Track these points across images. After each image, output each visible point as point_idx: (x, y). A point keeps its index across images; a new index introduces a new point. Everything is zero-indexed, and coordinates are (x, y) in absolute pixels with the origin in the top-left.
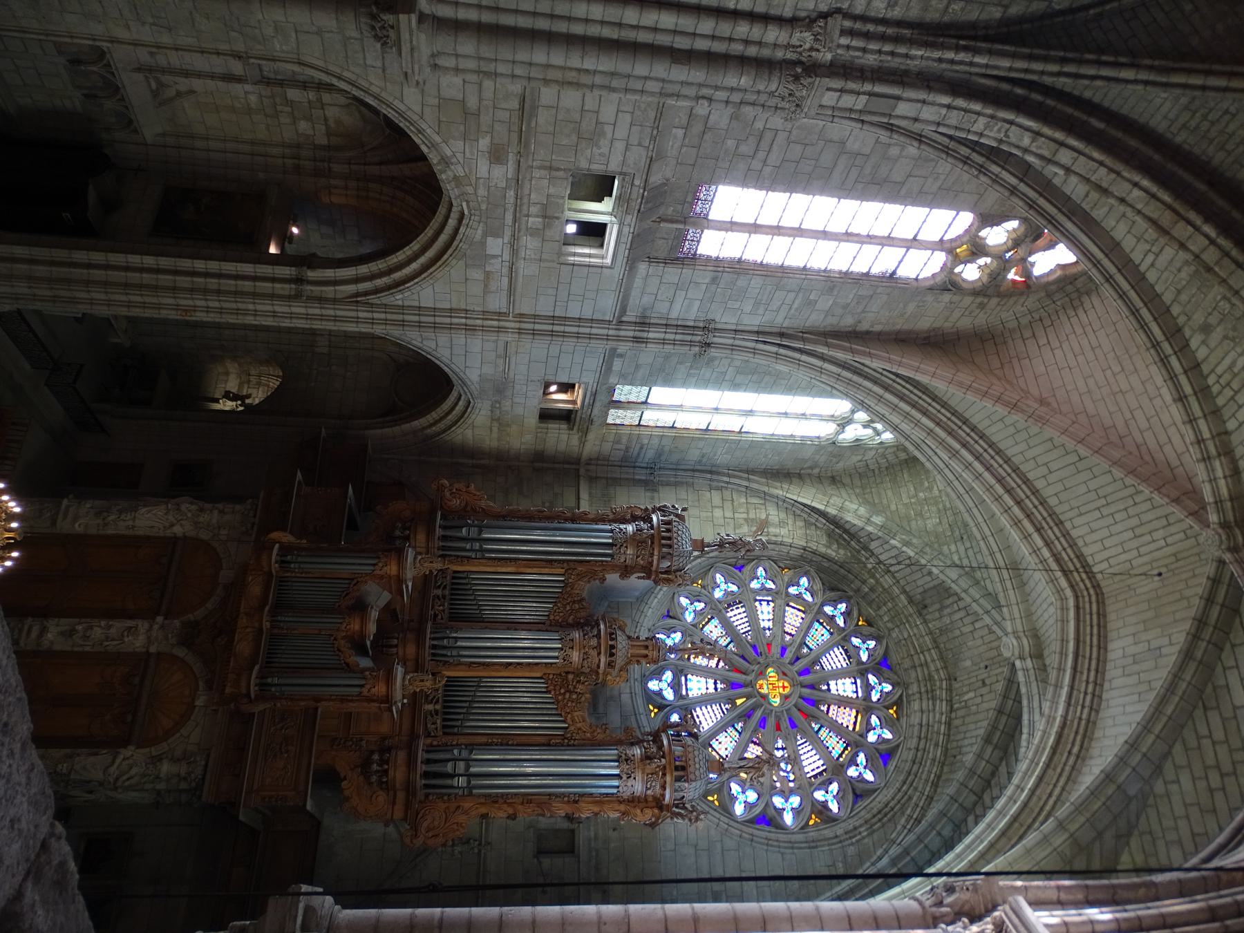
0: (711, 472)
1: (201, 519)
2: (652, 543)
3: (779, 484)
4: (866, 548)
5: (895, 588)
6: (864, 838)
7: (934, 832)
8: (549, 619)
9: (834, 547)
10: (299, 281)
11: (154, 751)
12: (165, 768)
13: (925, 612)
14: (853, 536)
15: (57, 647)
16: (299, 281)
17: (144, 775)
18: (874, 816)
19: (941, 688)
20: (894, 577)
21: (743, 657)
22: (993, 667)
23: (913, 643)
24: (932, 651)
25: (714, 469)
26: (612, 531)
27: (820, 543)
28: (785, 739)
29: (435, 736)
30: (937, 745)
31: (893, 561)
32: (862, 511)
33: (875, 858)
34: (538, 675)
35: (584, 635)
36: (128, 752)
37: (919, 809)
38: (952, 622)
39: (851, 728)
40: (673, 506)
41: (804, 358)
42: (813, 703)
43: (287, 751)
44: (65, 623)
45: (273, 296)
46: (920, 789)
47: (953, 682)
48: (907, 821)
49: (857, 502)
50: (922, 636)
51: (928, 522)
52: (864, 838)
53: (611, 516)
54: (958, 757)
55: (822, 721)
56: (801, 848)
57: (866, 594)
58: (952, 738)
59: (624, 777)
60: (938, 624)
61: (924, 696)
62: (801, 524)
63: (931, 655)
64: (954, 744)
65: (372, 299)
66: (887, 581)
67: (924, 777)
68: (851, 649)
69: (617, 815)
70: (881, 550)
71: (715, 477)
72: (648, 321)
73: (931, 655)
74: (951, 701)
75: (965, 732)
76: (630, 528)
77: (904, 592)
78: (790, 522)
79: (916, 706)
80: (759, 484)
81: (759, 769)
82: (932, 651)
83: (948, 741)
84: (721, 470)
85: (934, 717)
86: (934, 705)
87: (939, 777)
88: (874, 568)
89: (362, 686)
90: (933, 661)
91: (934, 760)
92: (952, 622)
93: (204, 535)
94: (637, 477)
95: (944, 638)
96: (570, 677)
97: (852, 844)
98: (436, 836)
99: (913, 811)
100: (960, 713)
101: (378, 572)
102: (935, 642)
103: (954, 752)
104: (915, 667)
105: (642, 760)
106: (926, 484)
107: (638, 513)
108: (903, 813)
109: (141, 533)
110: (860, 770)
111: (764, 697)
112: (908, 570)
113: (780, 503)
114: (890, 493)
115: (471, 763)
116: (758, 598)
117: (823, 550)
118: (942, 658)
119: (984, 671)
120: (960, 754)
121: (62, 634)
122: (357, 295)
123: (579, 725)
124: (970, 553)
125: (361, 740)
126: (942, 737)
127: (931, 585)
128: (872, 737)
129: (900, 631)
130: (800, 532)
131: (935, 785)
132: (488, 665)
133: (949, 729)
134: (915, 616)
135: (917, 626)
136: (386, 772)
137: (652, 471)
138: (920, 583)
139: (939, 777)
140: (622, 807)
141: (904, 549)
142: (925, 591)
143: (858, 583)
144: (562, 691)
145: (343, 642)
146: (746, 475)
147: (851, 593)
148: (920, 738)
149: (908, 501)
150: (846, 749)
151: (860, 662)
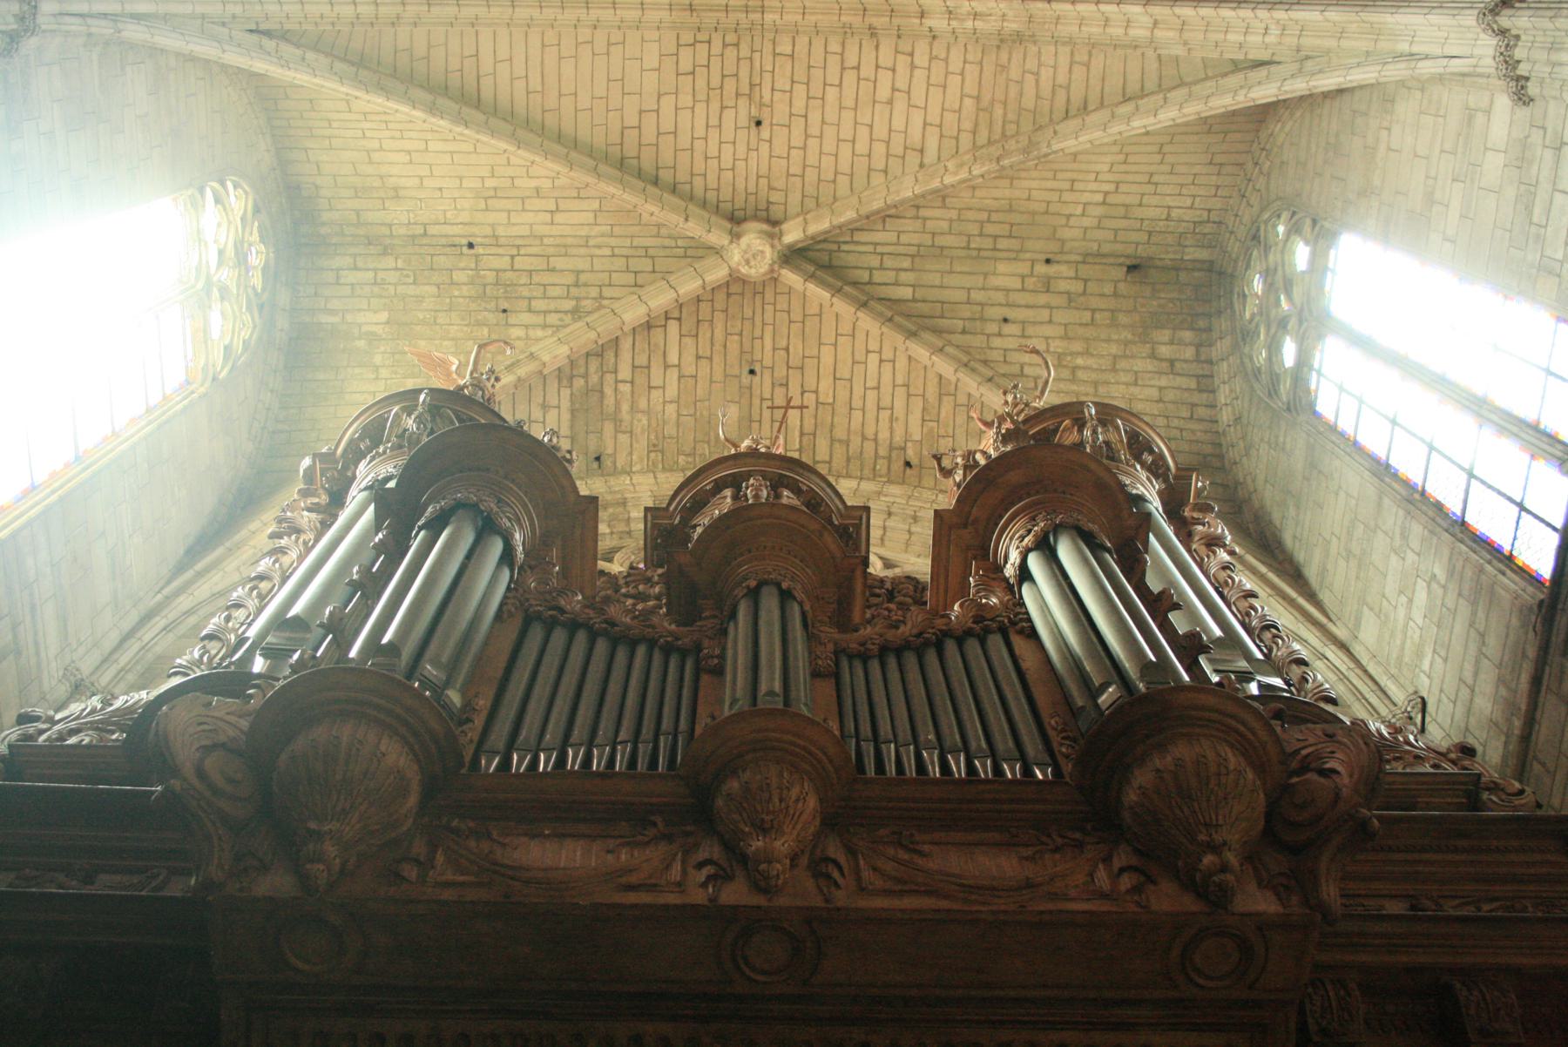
13: (607, 462)
22: (758, 356)
38: (648, 412)
54: (911, 454)
75: (864, 438)
103: (898, 466)
106: (361, 344)
119: (757, 379)
120: (904, 449)
124: (539, 305)
146: (189, 574)
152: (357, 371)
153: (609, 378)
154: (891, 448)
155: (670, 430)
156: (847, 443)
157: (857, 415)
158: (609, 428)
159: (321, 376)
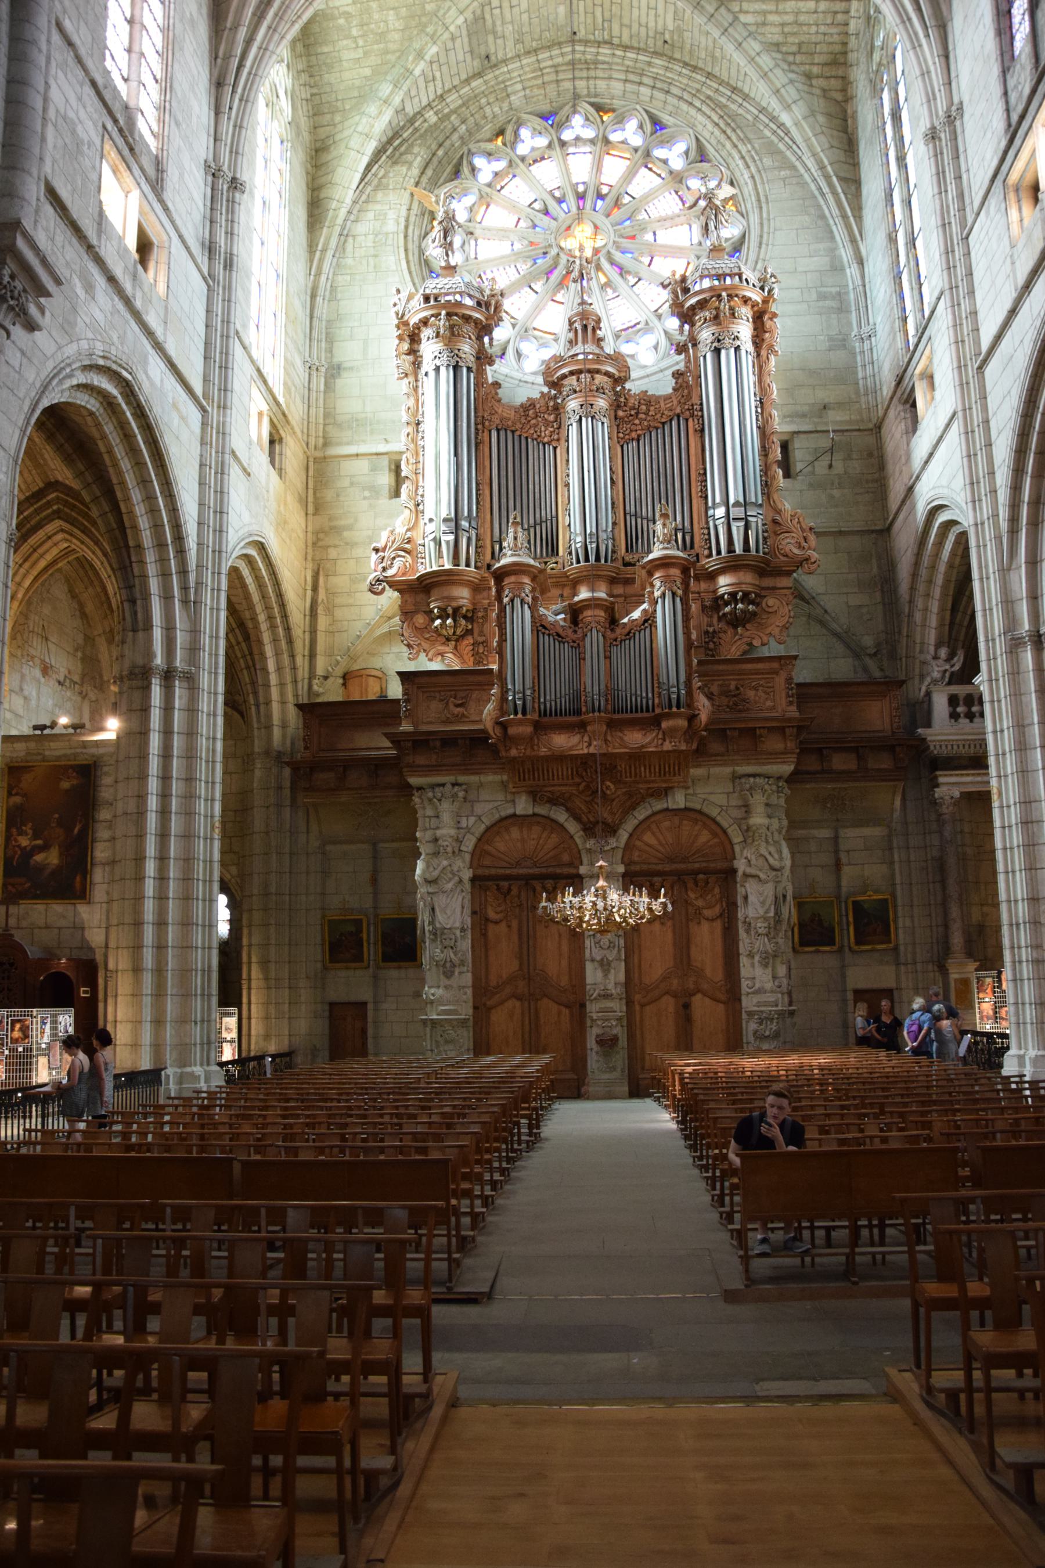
0: (313, 296)
1: (449, 849)
2: (456, 315)
3: (331, 213)
4: (412, 121)
5: (462, 92)
6: (753, 148)
7: (757, 59)
8: (549, 443)
9: (409, 157)
10: (168, 676)
11: (737, 838)
12: (758, 819)
13: (493, 58)
14: (396, 135)
15: (622, 977)
16: (168, 676)
17: (767, 842)
18: (729, 138)
19: (584, 53)
20: (449, 91)
21: (551, 272)
23: (529, 80)
24: (540, 57)
25: (309, 292)
26: (437, 369)
27: (406, 174)
28: (643, 230)
29: (697, 555)
30: (649, 64)
31: (431, 89)
32: (372, 109)
33: (773, 138)
34: (619, 449)
35: (575, 392)
36: (741, 865)
37: (721, 88)
38: (512, 22)
39: (628, 162)
40: (395, 305)
41: (248, 63)
42: (601, 196)
43: (737, 689)
44: (593, 975)
45: (192, 710)
46: (698, 86)
47: (577, 38)
48: (734, 102)
49: (357, 118)
50: (522, 67)
51: (391, 27)
52: (753, 148)
53: (411, 379)
54: (667, 37)
55: (622, 191)
56: (768, 212)
57: (467, 130)
58: (642, 45)
59: (738, 343)
60: (510, 44)
61: (592, 73)
62: (380, 195)
63: (544, 60)
64: (651, 42)
65: (192, 578)
66: (453, 100)
67: (685, 81)
68: (537, 155)
69: (772, 358)
70: (416, 100)
71: (320, 292)
72: (207, 243)
73: (544, 60)
74: (599, 42)
75: (640, 25)
76: (430, 349)
77: (467, 81)
78: (378, 207)
79: (602, 85)
80: (331, 236)
81: (717, 208)
82: (540, 57)
83: (645, 51)
84: (310, 285)
85: (617, 64)
86: (604, 63)
87: (686, 64)
88: (436, 113)
89: (674, 594)
90: (551, 58)
91: (667, 68)
92: (512, 22)
93: (469, 843)
94: (322, 387)
95: (527, 38)
96: (621, 413)
97: (761, 160)
98: (805, 539)
99: (723, 95)
100: (616, 31)
101: (529, 599)
102: (529, 52)
103: (660, 43)
104: (557, 81)
105: (719, 324)
106: (342, 21)
107: (406, 346)
108: (726, 106)
109: (468, 921)
110: (675, 155)
111: (596, 251)
112: (445, 68)
113: (352, 217)
114: (347, 75)
115: (732, 501)
116: (473, 256)
117: (415, 171)
118: (549, 48)
121: (606, 976)
122: (185, 602)
123: (675, 402)
125: (707, 632)
126: (640, 57)
127: (466, 40)
128: (637, 141)
129: (515, 93)
130: (392, 197)
131: (695, 68)
132: (613, 503)
133: (633, 48)
134: (497, 72)
135: (509, 72)
136: (746, 595)
137: (314, 368)
138: (461, 58)
139: (686, 64)
140: (763, 353)
141: (427, 58)
142: (471, 52)
143: (455, 137)
144: (637, 422)
145: (618, 631)
146: (318, 254)
147: (465, 149)
148: (640, 84)
149: (360, 51)
150: (650, 169)
151: (550, 146)
152: (345, 42)
153: (487, 8)
154: (656, 32)
155: (525, 29)
156: (630, 27)
157: (635, 11)
158: (491, 38)
159: (325, 49)
